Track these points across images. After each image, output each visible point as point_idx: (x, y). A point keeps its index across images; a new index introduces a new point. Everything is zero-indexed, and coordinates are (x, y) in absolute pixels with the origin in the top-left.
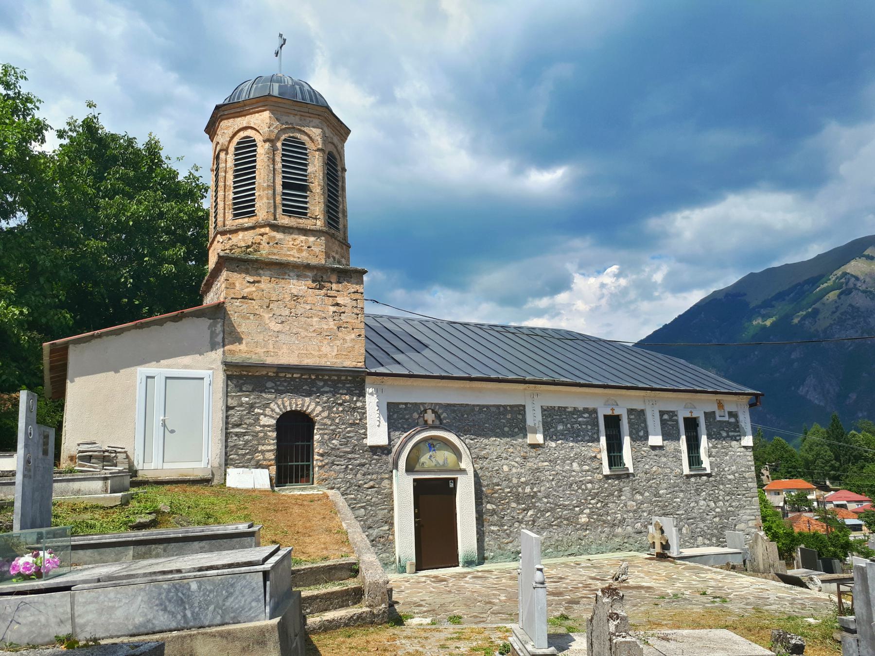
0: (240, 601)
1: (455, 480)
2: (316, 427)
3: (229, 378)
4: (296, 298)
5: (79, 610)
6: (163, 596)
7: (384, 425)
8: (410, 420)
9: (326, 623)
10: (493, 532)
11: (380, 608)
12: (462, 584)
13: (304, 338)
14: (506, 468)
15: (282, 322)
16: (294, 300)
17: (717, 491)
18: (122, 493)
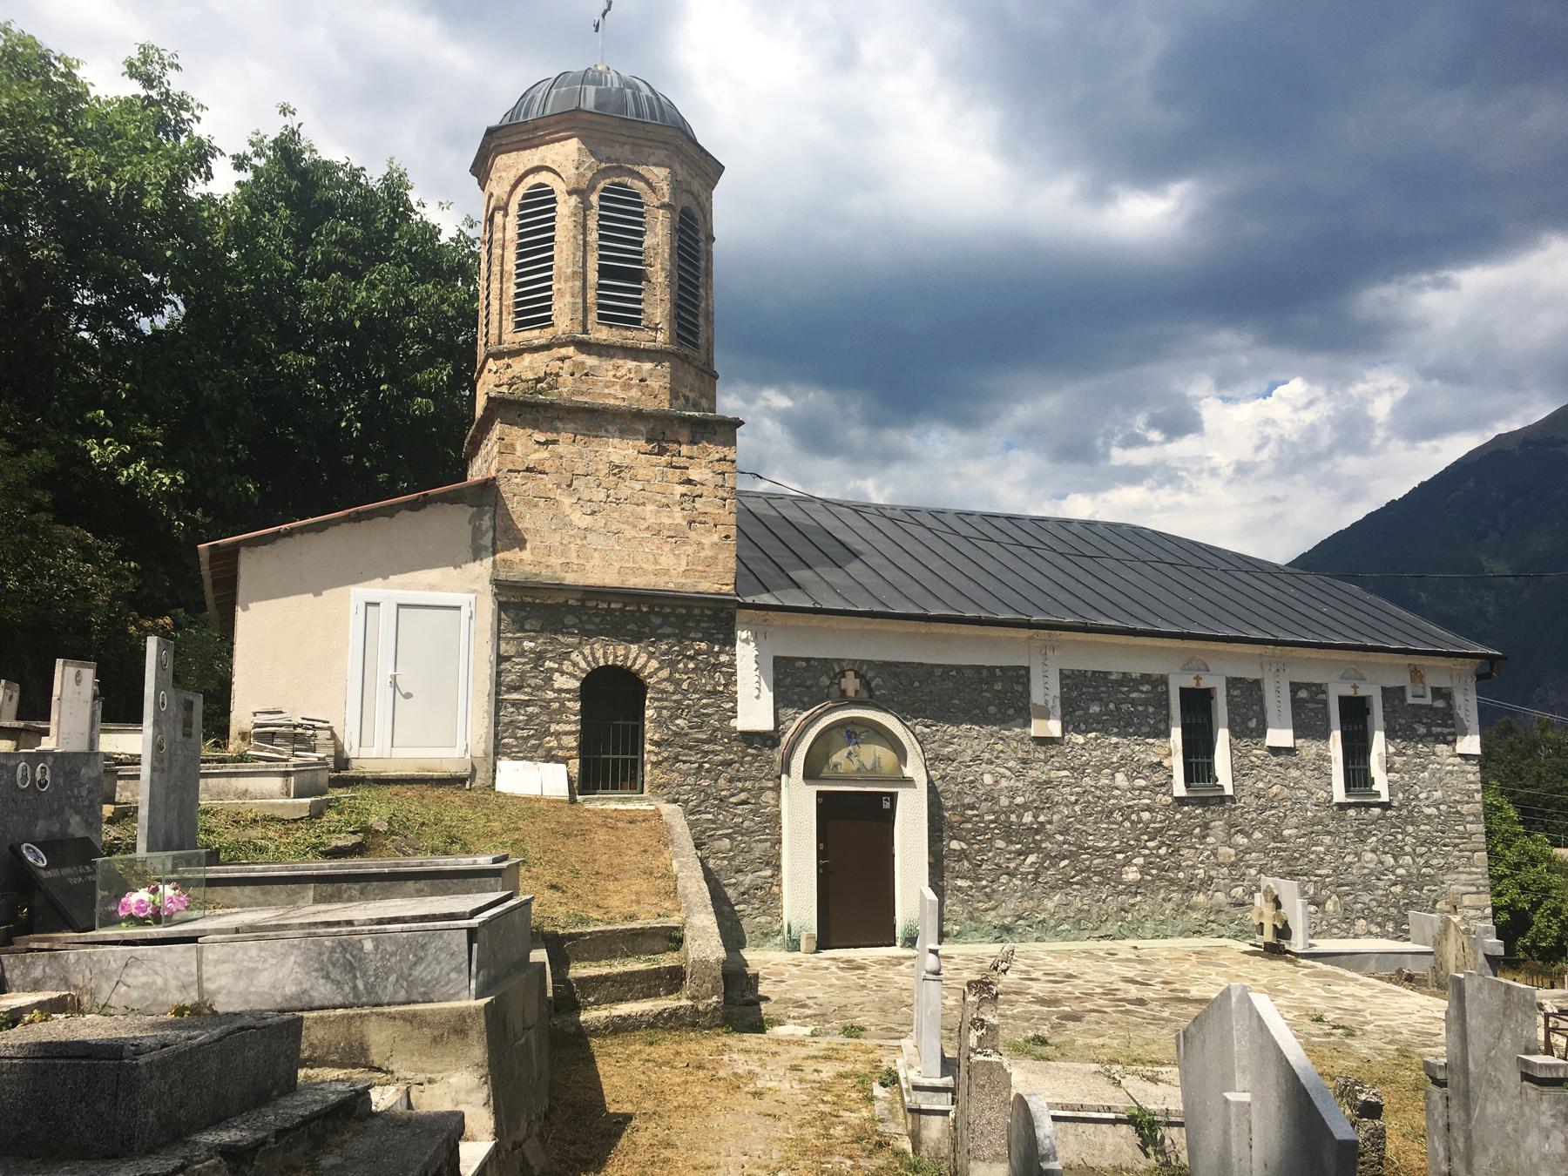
0: (433, 971)
1: (893, 797)
2: (648, 696)
3: (502, 607)
4: (617, 470)
5: (208, 971)
6: (325, 957)
7: (768, 696)
8: (814, 689)
9: (616, 1020)
10: (960, 889)
11: (710, 1002)
12: (890, 976)
13: (629, 540)
14: (988, 779)
15: (593, 513)
16: (615, 475)
17: (1400, 837)
18: (313, 799)
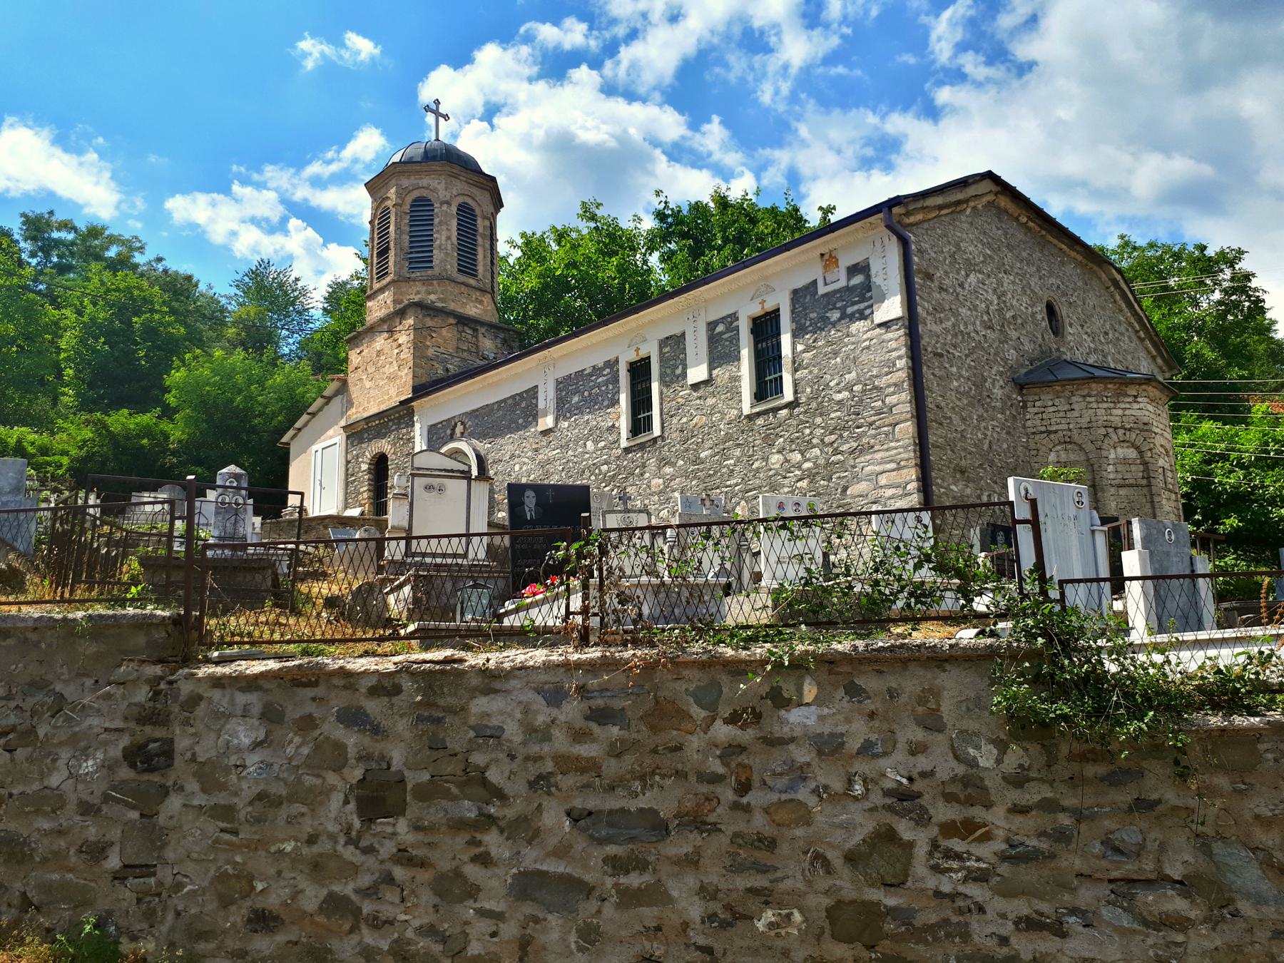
3: (348, 437)
4: (379, 353)
